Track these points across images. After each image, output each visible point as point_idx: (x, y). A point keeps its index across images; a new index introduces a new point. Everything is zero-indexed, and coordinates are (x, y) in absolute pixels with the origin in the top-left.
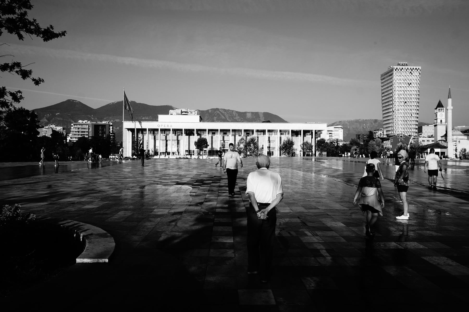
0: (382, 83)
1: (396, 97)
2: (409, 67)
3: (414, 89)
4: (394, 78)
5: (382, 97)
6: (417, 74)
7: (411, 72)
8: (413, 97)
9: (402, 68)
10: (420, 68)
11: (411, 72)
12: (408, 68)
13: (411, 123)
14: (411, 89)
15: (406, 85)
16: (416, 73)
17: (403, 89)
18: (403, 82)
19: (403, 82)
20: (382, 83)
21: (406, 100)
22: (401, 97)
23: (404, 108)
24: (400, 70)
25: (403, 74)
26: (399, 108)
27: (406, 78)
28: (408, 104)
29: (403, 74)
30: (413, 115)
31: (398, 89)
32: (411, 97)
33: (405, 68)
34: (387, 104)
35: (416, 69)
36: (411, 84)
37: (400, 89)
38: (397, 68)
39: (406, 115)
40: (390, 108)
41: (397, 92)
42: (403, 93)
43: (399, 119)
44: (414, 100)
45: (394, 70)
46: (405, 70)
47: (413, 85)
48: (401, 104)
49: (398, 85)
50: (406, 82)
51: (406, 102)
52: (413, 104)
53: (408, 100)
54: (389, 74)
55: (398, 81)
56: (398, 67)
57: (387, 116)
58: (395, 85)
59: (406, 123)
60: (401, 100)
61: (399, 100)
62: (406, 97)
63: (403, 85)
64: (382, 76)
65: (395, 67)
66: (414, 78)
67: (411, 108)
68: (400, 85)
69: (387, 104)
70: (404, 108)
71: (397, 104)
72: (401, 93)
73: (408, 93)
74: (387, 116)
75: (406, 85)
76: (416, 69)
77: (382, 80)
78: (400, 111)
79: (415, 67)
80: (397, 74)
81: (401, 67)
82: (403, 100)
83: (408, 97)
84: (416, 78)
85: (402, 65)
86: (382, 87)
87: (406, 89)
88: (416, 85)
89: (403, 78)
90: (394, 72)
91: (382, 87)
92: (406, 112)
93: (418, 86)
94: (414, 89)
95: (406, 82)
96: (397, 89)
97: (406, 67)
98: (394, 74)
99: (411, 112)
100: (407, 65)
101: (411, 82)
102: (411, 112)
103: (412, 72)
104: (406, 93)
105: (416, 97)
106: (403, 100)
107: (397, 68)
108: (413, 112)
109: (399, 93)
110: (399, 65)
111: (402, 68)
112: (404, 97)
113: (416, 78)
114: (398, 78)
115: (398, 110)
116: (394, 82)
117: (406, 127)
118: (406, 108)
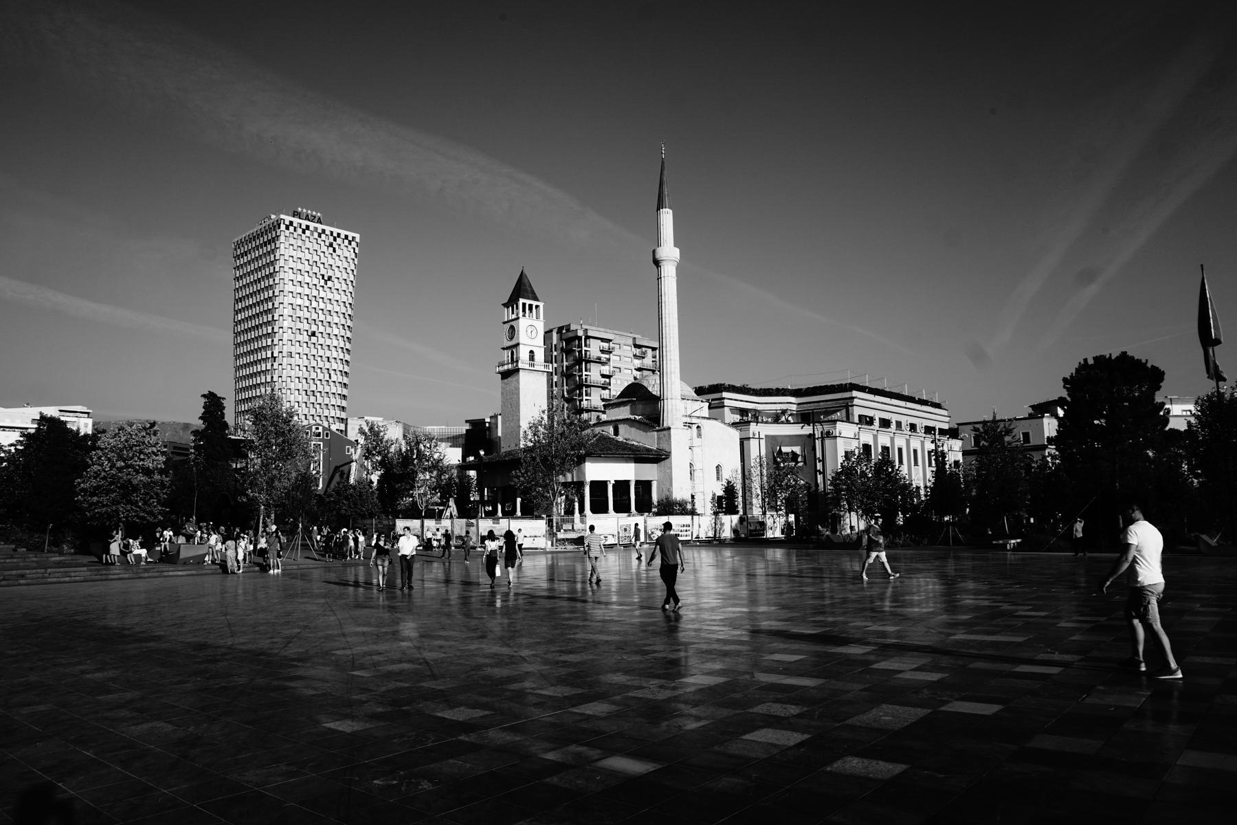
0: (237, 268)
1: (286, 312)
2: (328, 229)
3: (339, 296)
4: (282, 251)
5: (237, 312)
6: (347, 254)
7: (331, 245)
8: (336, 320)
9: (308, 227)
10: (357, 236)
11: (331, 245)
12: (324, 231)
13: (327, 401)
14: (330, 296)
15: (315, 281)
16: (346, 252)
17: (307, 291)
18: (308, 268)
19: (308, 268)
20: (237, 268)
21: (314, 328)
22: (300, 314)
23: (307, 351)
24: (299, 231)
25: (308, 245)
26: (293, 349)
27: (317, 258)
28: (321, 341)
29: (308, 245)
30: (334, 378)
31: (292, 288)
32: (329, 319)
33: (316, 229)
34: (253, 335)
35: (346, 237)
36: (330, 278)
37: (299, 290)
38: (291, 223)
39: (313, 375)
40: (265, 348)
41: (288, 299)
42: (307, 303)
43: (292, 386)
44: (336, 331)
45: (283, 227)
46: (316, 235)
47: (338, 286)
48: (299, 338)
49: (292, 277)
50: (316, 270)
51: (314, 334)
52: (335, 343)
53: (322, 329)
54: (268, 237)
55: (292, 264)
56: (296, 221)
57: (251, 376)
58: (282, 275)
59: (313, 399)
60: (299, 325)
61: (292, 324)
62: (315, 316)
63: (308, 280)
64: (239, 245)
65: (288, 219)
66: (339, 264)
67: (328, 354)
68: (300, 278)
69: (253, 335)
70: (307, 351)
71: (286, 337)
72: (299, 301)
73: (322, 306)
74: (251, 376)
75: (315, 281)
76: (346, 237)
77: (238, 257)
78: (296, 360)
79: (343, 233)
80: (292, 241)
81: (305, 223)
82: (307, 327)
83: (322, 317)
84: (346, 265)
85: (307, 218)
86: (237, 279)
87: (315, 293)
88: (344, 287)
89: (309, 257)
90: (283, 233)
91: (237, 279)
92: (314, 363)
93: (351, 289)
94: (337, 297)
95: (316, 270)
96: (289, 287)
97: (320, 227)
98: (282, 239)
99: (328, 365)
100: (319, 222)
101: (331, 273)
102: (328, 365)
103: (335, 245)
104: (314, 304)
105: (343, 321)
106: (307, 327)
107: (291, 223)
108: (335, 366)
109: (292, 301)
110: (296, 214)
111: (308, 227)
112: (307, 315)
113: (346, 265)
114: (294, 254)
115: (290, 355)
116: (282, 263)
117: (313, 411)
118: (314, 352)
